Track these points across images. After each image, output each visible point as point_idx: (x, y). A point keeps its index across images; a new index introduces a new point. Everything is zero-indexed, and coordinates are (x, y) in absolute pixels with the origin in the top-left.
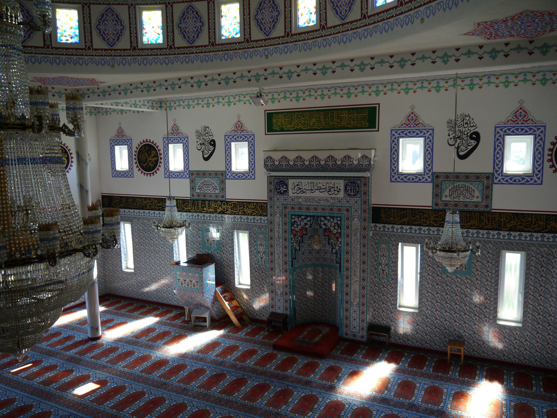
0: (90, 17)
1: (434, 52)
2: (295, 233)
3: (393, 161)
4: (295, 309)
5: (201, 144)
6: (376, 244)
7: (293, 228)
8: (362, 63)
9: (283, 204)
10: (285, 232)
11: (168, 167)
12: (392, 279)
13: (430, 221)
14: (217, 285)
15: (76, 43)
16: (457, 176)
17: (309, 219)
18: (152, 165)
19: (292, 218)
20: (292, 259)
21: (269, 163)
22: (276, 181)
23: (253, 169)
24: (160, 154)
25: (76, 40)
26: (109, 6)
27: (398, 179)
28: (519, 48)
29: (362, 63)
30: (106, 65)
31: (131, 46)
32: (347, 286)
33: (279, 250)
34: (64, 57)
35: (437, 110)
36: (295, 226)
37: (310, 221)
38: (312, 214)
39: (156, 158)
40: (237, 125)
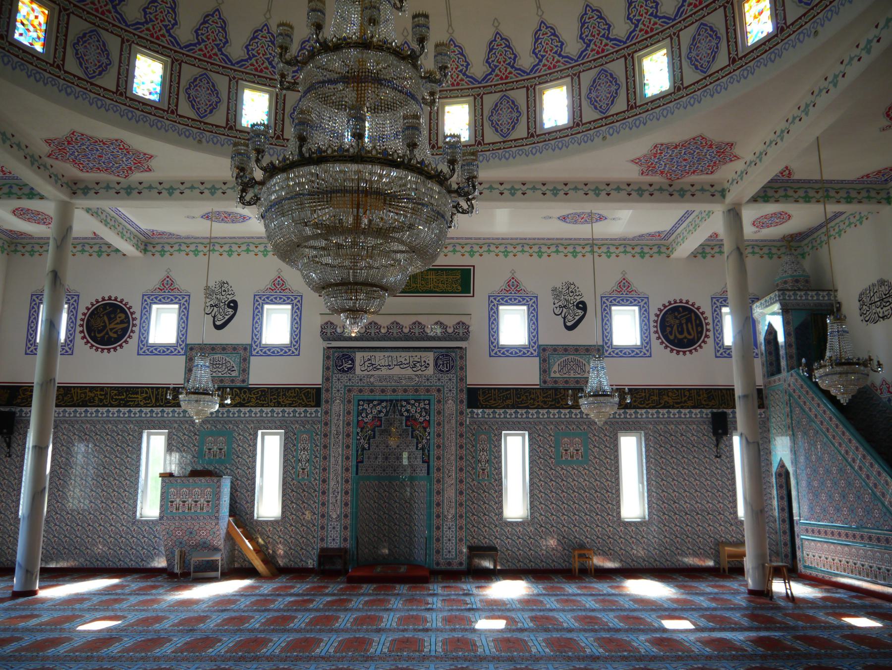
0: (179, 76)
1: (586, 185)
2: (363, 425)
5: (211, 306)
6: (473, 435)
7: (360, 418)
8: (513, 188)
10: (348, 424)
15: (154, 101)
16: (566, 349)
17: (384, 404)
18: (115, 336)
19: (359, 405)
23: (297, 342)
25: (155, 97)
26: (205, 71)
28: (661, 190)
29: (513, 188)
30: (191, 138)
31: (227, 124)
32: (438, 493)
33: (337, 453)
34: (138, 113)
35: (541, 277)
36: (364, 415)
37: (386, 407)
38: (388, 398)
39: (125, 325)
40: (276, 282)
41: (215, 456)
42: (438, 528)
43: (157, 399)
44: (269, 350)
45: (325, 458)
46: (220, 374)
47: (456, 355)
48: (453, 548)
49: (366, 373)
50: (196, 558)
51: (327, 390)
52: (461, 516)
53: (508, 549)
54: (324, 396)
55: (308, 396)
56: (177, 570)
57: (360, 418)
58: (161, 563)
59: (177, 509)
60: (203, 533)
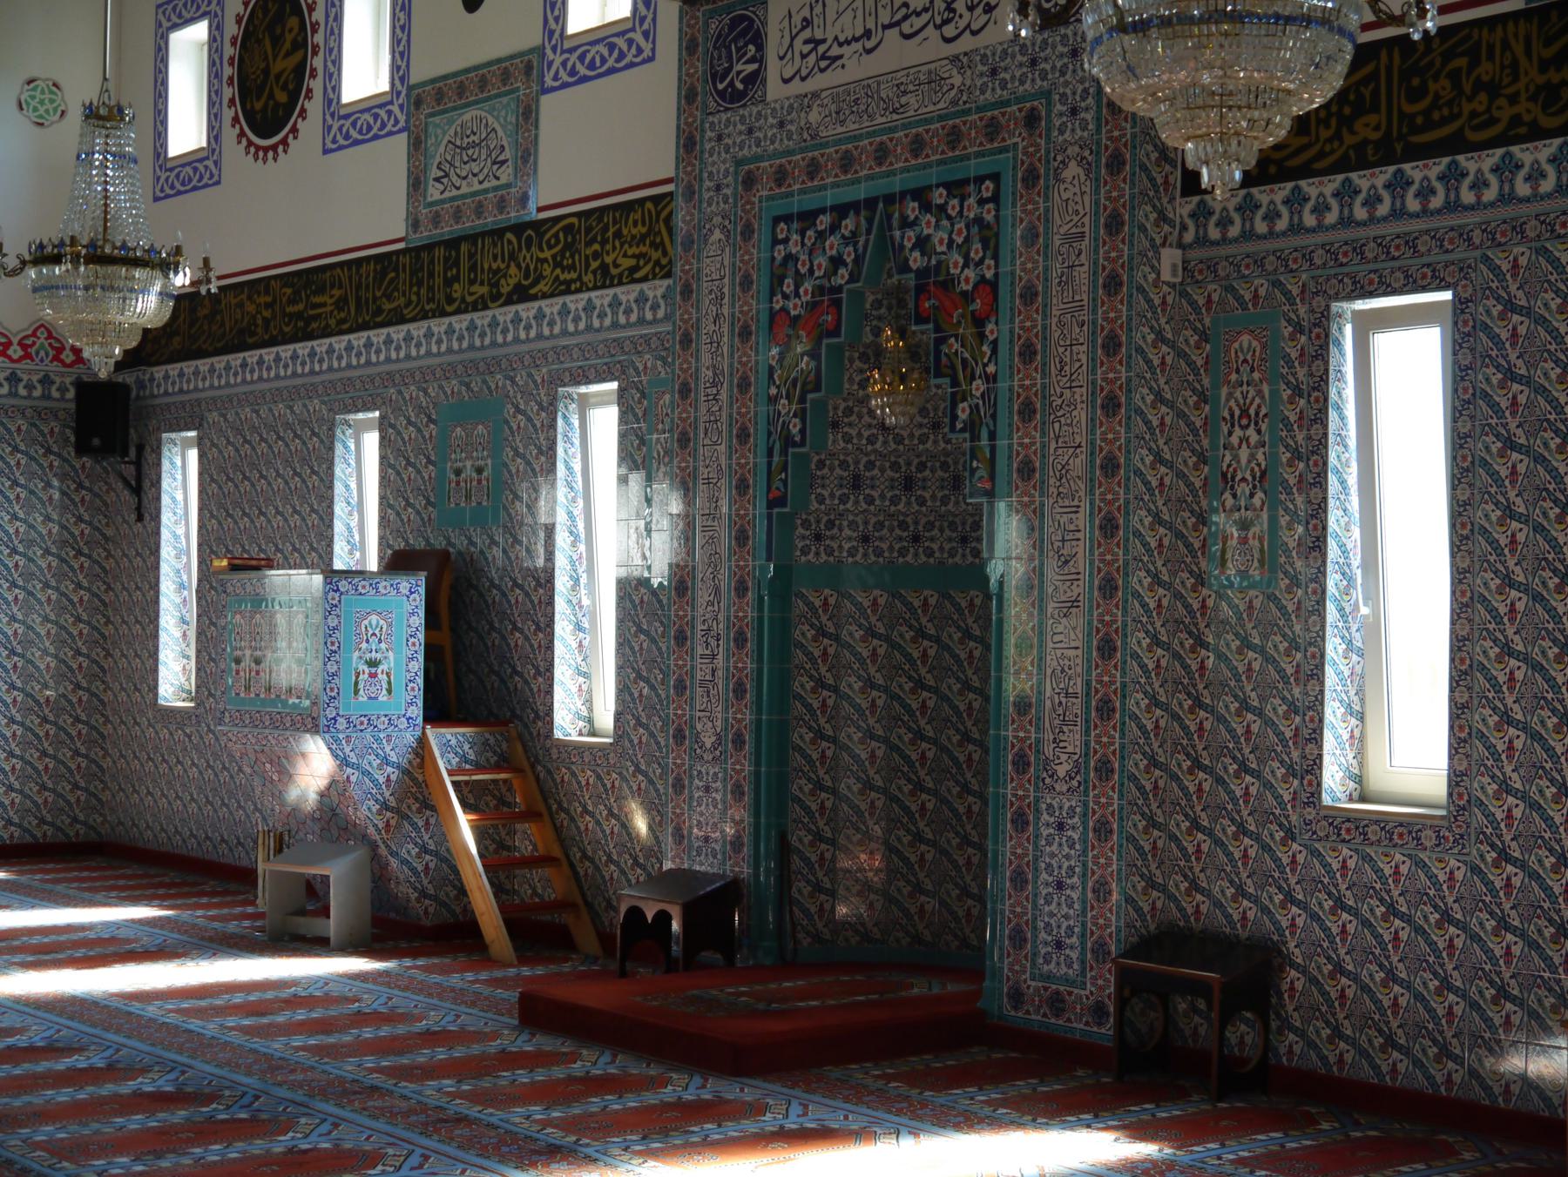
4: (784, 849)
11: (337, 89)
13: (1513, 99)
14: (438, 710)
17: (849, 224)
37: (851, 239)
38: (861, 192)
53: (1339, 969)
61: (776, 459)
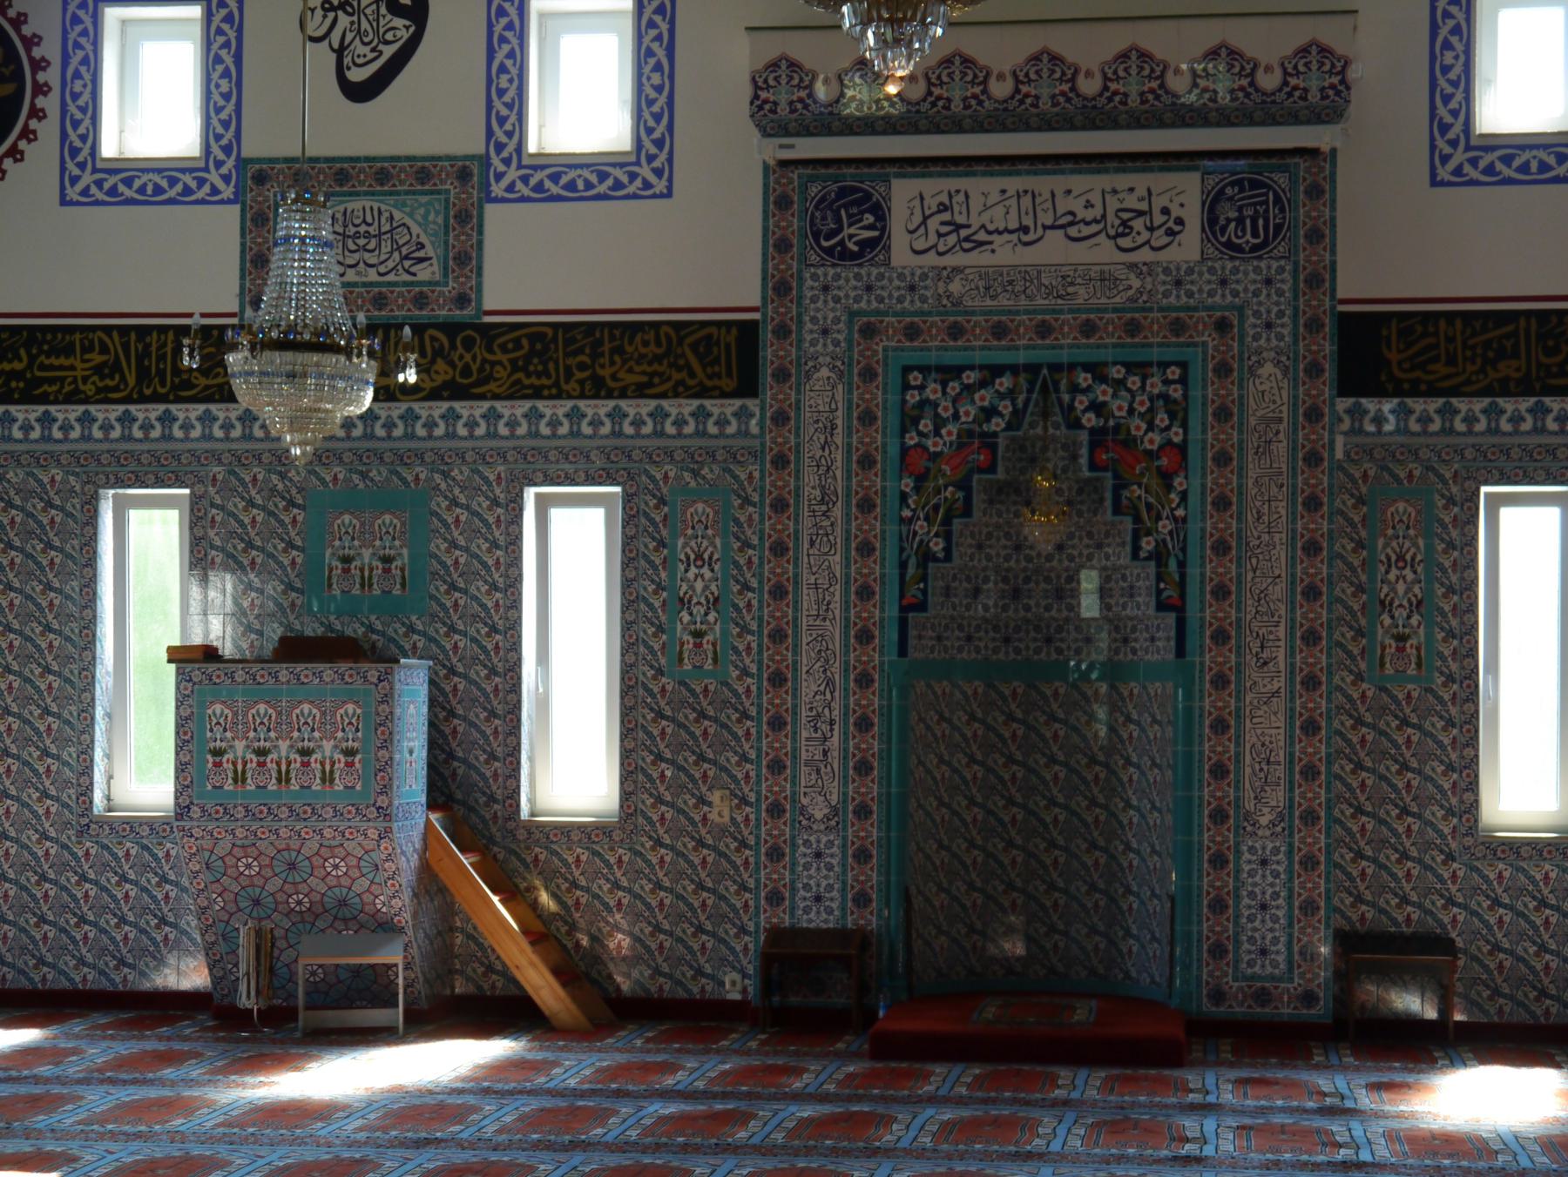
2: (924, 463)
3: (1442, 82)
6: (1361, 501)
7: (912, 439)
9: (853, 314)
10: (867, 462)
11: (92, 136)
12: (1451, 679)
17: (1005, 382)
19: (906, 387)
20: (903, 609)
21: (782, 96)
22: (814, 189)
23: (659, 143)
24: (39, 65)
27: (1467, 168)
32: (1220, 726)
33: (823, 571)
36: (926, 425)
37: (1011, 394)
38: (1021, 357)
39: (8, 89)
41: (366, 584)
42: (1219, 861)
43: (143, 375)
44: (555, 178)
45: (779, 592)
46: (372, 276)
47: (1293, 181)
48: (1280, 945)
49: (931, 259)
50: (315, 957)
51: (782, 332)
52: (1310, 818)
53: (1497, 948)
54: (770, 353)
55: (707, 356)
56: (246, 999)
57: (912, 439)
58: (188, 974)
59: (240, 779)
60: (337, 868)
61: (911, 570)
